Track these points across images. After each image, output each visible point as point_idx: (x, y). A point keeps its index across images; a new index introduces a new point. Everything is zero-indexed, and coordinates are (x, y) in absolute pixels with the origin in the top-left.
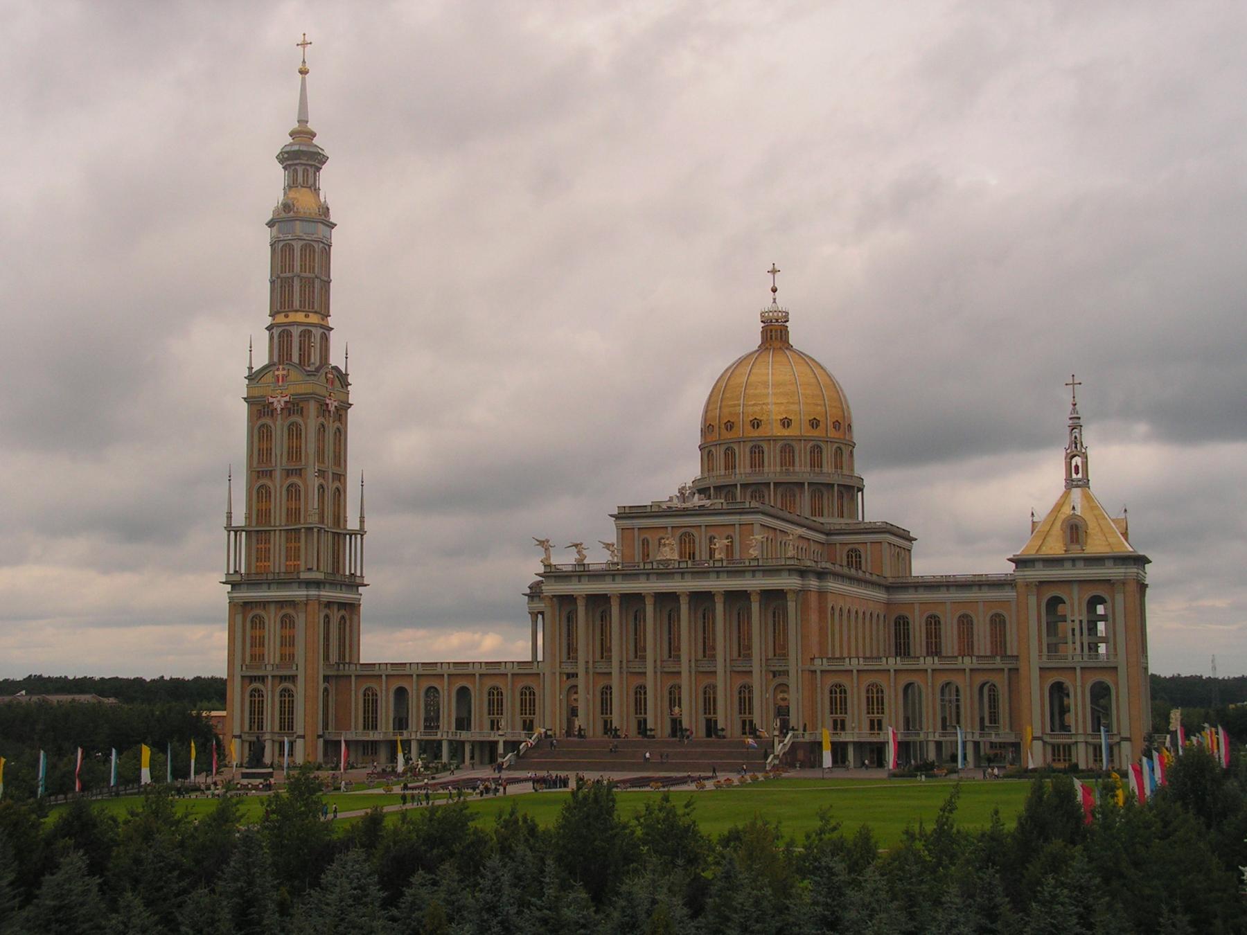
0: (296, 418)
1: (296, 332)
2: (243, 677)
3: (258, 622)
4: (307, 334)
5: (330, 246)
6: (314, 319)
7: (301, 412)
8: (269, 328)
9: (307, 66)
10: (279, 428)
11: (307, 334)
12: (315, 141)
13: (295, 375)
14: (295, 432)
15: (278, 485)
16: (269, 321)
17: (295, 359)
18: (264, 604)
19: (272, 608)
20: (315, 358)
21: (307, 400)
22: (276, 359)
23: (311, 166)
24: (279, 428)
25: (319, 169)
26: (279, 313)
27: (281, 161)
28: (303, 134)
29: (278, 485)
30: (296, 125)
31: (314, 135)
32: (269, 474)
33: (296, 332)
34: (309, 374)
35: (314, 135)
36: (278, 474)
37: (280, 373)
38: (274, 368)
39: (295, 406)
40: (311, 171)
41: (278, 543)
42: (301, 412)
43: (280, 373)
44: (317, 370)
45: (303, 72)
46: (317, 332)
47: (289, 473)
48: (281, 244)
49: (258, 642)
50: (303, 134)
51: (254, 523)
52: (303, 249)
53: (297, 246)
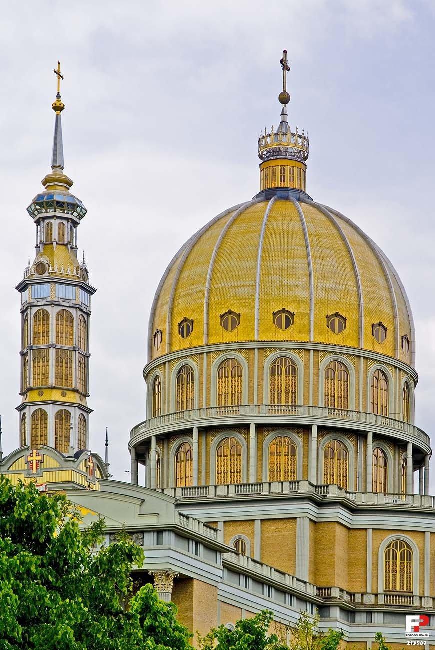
1: (52, 411)
4: (64, 416)
5: (89, 315)
6: (73, 398)
8: (20, 409)
9: (63, 101)
11: (64, 416)
12: (73, 191)
13: (50, 461)
16: (20, 400)
17: (51, 443)
20: (74, 444)
22: (28, 443)
23: (68, 219)
25: (75, 224)
26: (31, 390)
27: (32, 214)
28: (57, 180)
30: (50, 172)
31: (70, 184)
33: (52, 411)
34: (67, 460)
35: (70, 184)
37: (35, 459)
38: (28, 453)
40: (68, 225)
43: (35, 459)
44: (77, 456)
45: (59, 108)
46: (76, 414)
48: (35, 310)
50: (57, 180)
52: (60, 316)
53: (53, 312)
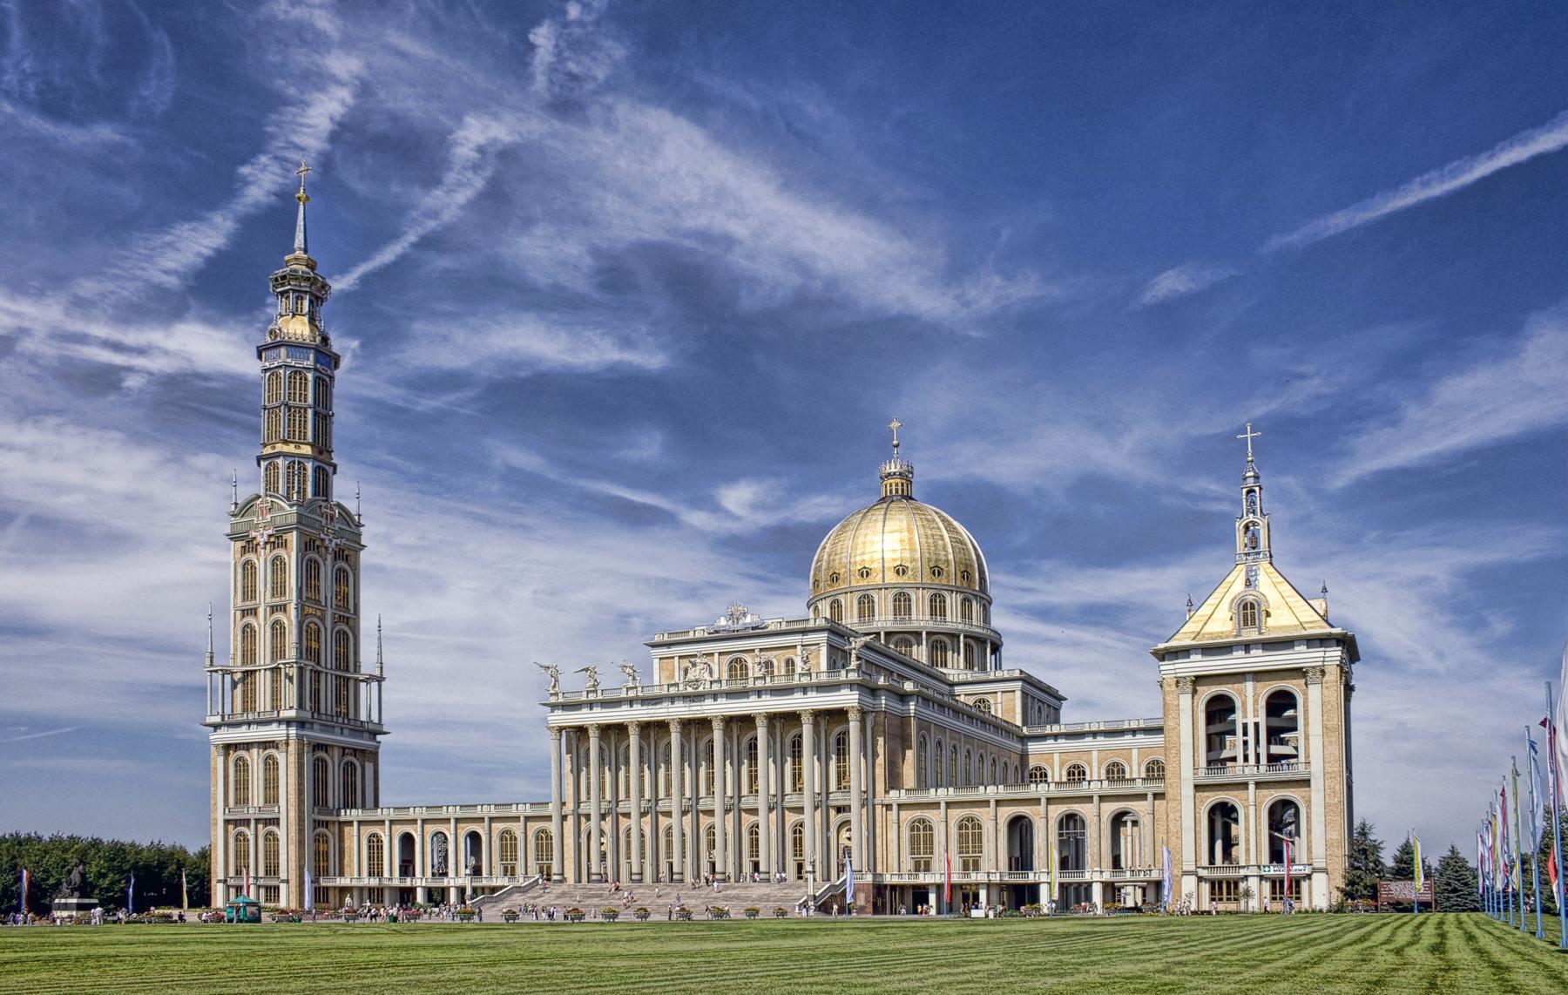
0: (277, 552)
2: (227, 822)
3: (242, 766)
7: (284, 545)
10: (261, 560)
14: (278, 565)
15: (261, 623)
18: (247, 746)
19: (255, 751)
21: (290, 531)
24: (261, 560)
29: (261, 623)
32: (253, 612)
36: (261, 612)
39: (277, 541)
41: (263, 681)
42: (284, 545)
47: (274, 609)
49: (242, 786)
51: (239, 661)
